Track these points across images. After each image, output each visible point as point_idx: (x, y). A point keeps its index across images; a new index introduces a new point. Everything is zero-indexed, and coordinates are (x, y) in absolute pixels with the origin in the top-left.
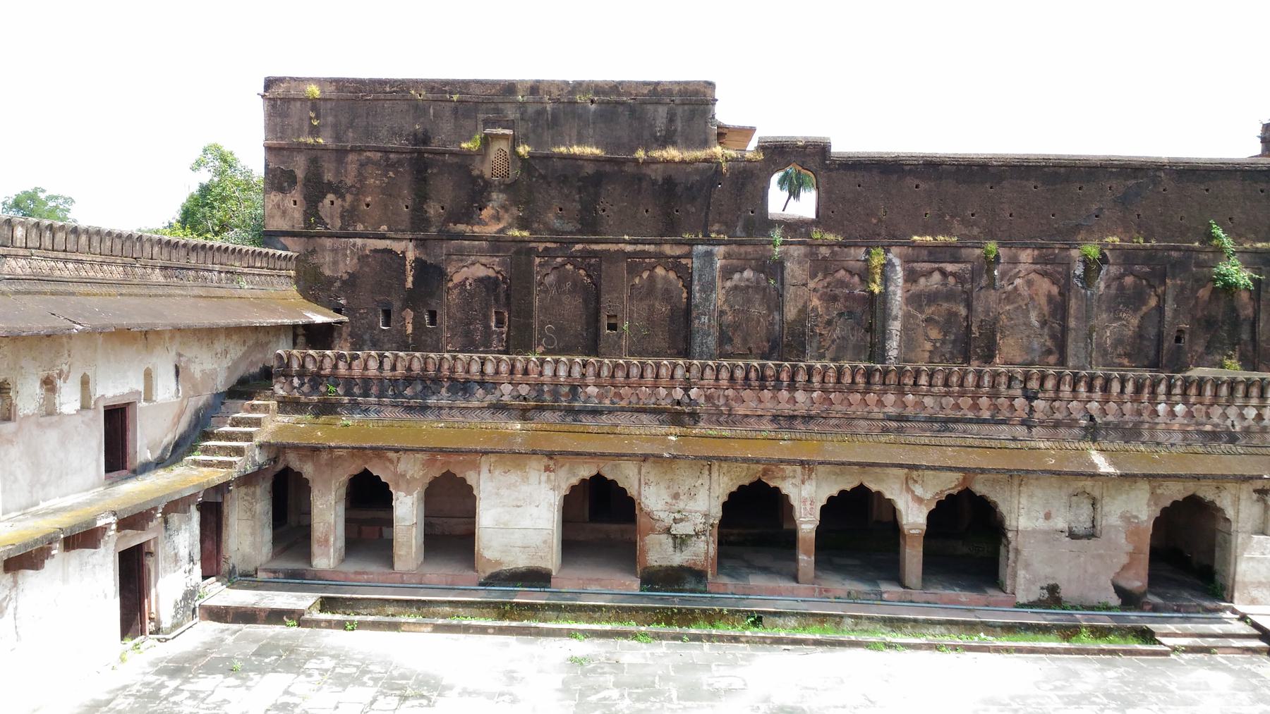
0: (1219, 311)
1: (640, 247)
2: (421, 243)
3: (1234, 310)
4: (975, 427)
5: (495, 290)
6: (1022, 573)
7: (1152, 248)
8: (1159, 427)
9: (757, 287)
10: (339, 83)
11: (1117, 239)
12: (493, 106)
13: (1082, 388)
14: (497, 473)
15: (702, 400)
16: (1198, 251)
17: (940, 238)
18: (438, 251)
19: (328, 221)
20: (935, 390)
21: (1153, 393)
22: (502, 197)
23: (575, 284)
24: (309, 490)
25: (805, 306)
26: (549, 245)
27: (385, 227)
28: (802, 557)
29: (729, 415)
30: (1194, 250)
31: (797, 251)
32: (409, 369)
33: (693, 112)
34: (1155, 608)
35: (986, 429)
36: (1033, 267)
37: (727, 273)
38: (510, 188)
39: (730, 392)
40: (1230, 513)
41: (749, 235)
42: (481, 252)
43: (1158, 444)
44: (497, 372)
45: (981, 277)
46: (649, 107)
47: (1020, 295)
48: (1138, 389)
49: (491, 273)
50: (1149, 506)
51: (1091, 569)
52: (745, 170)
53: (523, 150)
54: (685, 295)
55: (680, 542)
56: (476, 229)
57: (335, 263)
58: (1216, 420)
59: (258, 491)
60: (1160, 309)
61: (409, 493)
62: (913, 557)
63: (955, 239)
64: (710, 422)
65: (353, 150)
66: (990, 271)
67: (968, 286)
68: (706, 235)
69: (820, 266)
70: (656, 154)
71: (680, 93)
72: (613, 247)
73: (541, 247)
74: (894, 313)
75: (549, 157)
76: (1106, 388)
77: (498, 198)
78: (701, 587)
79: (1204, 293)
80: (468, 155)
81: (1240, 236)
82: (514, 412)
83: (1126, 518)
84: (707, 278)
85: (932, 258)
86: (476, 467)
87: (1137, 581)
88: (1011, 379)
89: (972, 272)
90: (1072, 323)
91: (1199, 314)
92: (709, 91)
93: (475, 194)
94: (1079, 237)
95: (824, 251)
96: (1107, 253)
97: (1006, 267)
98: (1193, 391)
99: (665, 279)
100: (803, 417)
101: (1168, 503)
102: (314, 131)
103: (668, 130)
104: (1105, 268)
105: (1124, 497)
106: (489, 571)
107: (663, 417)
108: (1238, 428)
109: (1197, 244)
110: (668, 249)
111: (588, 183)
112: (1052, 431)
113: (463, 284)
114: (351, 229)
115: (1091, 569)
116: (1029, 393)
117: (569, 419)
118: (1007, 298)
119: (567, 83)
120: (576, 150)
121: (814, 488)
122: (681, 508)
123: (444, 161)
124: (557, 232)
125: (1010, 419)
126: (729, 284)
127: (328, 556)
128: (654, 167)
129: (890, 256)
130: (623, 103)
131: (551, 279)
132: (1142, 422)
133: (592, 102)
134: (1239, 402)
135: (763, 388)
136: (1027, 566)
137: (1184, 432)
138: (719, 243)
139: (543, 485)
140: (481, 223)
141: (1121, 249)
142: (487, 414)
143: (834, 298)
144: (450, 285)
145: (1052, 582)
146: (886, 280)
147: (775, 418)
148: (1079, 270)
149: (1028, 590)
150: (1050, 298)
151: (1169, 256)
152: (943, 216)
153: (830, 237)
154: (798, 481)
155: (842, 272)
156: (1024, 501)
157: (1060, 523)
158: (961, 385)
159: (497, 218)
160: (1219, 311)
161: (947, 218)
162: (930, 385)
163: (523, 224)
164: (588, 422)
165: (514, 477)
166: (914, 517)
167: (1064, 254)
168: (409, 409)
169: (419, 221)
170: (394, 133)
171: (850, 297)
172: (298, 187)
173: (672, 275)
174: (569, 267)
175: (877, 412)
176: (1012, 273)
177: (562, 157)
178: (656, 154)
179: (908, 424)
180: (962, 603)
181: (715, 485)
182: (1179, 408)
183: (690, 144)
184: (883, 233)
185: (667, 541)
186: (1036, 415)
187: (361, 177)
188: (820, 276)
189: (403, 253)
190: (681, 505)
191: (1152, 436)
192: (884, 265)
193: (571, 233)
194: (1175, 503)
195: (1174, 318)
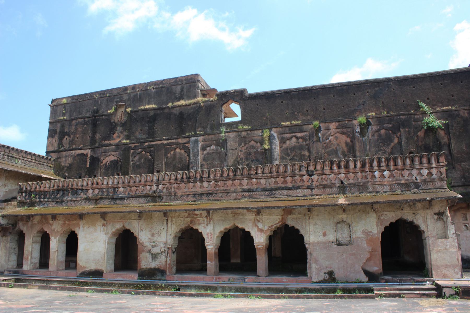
0: (430, 141)
1: (170, 141)
2: (93, 149)
3: (437, 140)
4: (285, 192)
5: (117, 165)
6: (314, 265)
7: (391, 116)
8: (377, 183)
9: (217, 152)
10: (72, 97)
11: (374, 114)
12: (119, 96)
13: (335, 167)
14: (85, 228)
15: (165, 190)
16: (414, 114)
17: (293, 122)
18: (98, 152)
19: (65, 145)
20: (265, 175)
21: (371, 166)
22: (121, 128)
23: (145, 159)
24: (24, 237)
25: (237, 158)
26: (136, 144)
27: (82, 145)
28: (208, 262)
29: (175, 195)
30: (411, 114)
31: (232, 135)
32: (59, 186)
33: (190, 86)
34: (387, 281)
35: (291, 192)
36: (337, 130)
37: (204, 148)
38: (124, 125)
39: (175, 185)
40: (423, 227)
41: (212, 130)
42: (113, 151)
43: (377, 192)
44: (87, 185)
45: (313, 137)
46: (174, 87)
47: (332, 144)
48: (363, 165)
49: (116, 158)
50: (377, 225)
51: (350, 262)
52: (210, 105)
53: (129, 110)
54: (188, 159)
55: (155, 256)
56: (111, 142)
57: (66, 161)
58: (406, 177)
59: (9, 239)
60: (400, 143)
61: (55, 238)
62: (262, 261)
63: (299, 122)
64: (167, 200)
65: (75, 119)
66: (317, 134)
67: (308, 142)
68: (195, 133)
69: (243, 140)
70: (177, 104)
71: (186, 80)
72: (159, 142)
73: (133, 145)
74: (275, 157)
75: (137, 111)
76: (347, 167)
77: (119, 129)
78: (163, 278)
79: (421, 134)
80: (110, 115)
81: (434, 105)
82: (93, 201)
83: (366, 233)
84: (195, 150)
85: (291, 131)
86: (78, 225)
87: (376, 267)
89: (309, 135)
91: (420, 144)
92: (196, 77)
93: (112, 128)
94: (356, 115)
95: (244, 134)
96: (370, 120)
97: (324, 132)
98: (392, 163)
99: (180, 153)
100: (206, 194)
101: (388, 224)
102: (64, 115)
103: (181, 94)
104: (370, 127)
105: (363, 222)
106: (81, 271)
107: (149, 199)
108: (418, 181)
109: (413, 111)
110: (180, 141)
111: (150, 119)
112: (322, 190)
113: (106, 164)
114: (71, 147)
115: (350, 262)
116: (310, 173)
117: (112, 203)
118: (327, 146)
119: (145, 83)
120: (147, 107)
121: (212, 228)
122: (157, 241)
123: (103, 119)
124: (139, 139)
125: (301, 186)
126: (205, 152)
127: (27, 264)
128: (175, 109)
129: (272, 132)
130: (165, 87)
131: (137, 158)
132: (368, 182)
133: (154, 88)
134: (417, 166)
135: (189, 182)
136: (316, 261)
137: (391, 185)
138: (200, 135)
139: (102, 232)
140: (114, 139)
141: (376, 118)
142: (83, 203)
143: (250, 154)
144: (102, 164)
145: (330, 270)
146: (271, 143)
147: (194, 195)
148: (358, 129)
149: (318, 274)
150: (347, 144)
151: (400, 118)
152: (294, 113)
153: (246, 127)
154: (205, 225)
155: (252, 142)
156: (312, 227)
157: (331, 237)
158: (277, 172)
159: (119, 137)
160: (430, 141)
161: (296, 113)
162: (263, 173)
163: (127, 138)
164: (119, 203)
165: (91, 229)
166: (260, 240)
167: (350, 123)
168: (58, 202)
169: (93, 141)
170: (88, 111)
171: (257, 152)
172: (57, 135)
173: (183, 151)
174: (144, 153)
175: (239, 189)
176: (327, 134)
177: (142, 110)
178: (177, 104)
179: (254, 193)
180: (284, 282)
181: (169, 229)
182: (386, 173)
183: (189, 98)
184: (268, 123)
185: (149, 256)
186: (314, 183)
187: (76, 128)
188: (243, 144)
189: (87, 154)
190: (155, 239)
191: (374, 188)
192: (269, 137)
193: (144, 139)
194: (391, 224)
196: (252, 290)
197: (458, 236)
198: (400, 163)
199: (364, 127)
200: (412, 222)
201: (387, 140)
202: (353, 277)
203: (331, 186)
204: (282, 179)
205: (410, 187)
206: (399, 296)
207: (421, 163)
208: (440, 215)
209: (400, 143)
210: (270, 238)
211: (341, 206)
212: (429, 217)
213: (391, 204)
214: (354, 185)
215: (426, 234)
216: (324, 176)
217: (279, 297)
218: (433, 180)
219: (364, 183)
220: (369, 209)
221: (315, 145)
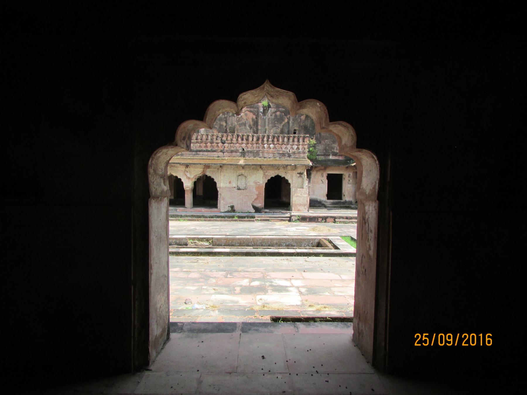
0: (308, 123)
4: (206, 153)
6: (222, 202)
13: (240, 139)
21: (263, 140)
34: (266, 213)
35: (209, 153)
40: (290, 181)
43: (265, 158)
48: (258, 139)
51: (244, 200)
58: (284, 150)
60: (288, 122)
62: (189, 198)
67: (226, 116)
76: (247, 140)
83: (256, 183)
87: (260, 204)
88: (217, 137)
90: (259, 128)
91: (302, 124)
98: (276, 140)
101: (269, 178)
105: (255, 175)
112: (231, 154)
134: (291, 143)
136: (223, 199)
145: (232, 205)
148: (262, 110)
149: (224, 207)
150: (253, 120)
156: (222, 177)
157: (234, 185)
158: (201, 139)
166: (188, 185)
182: (272, 146)
194: (272, 178)
195: (293, 125)
196: (181, 216)
197: (309, 187)
198: (281, 140)
199: (266, 109)
200: (284, 178)
201: (280, 120)
202: (246, 209)
203: (236, 151)
204: (204, 144)
205: (285, 156)
206: (268, 220)
207: (293, 141)
208: (301, 174)
209: (288, 122)
210: (195, 183)
211: (240, 165)
212: (294, 175)
213: (273, 167)
214: (251, 152)
215: (291, 186)
216: (232, 145)
217: (198, 221)
218: (299, 153)
219: (257, 151)
220: (259, 168)
221: (230, 118)
